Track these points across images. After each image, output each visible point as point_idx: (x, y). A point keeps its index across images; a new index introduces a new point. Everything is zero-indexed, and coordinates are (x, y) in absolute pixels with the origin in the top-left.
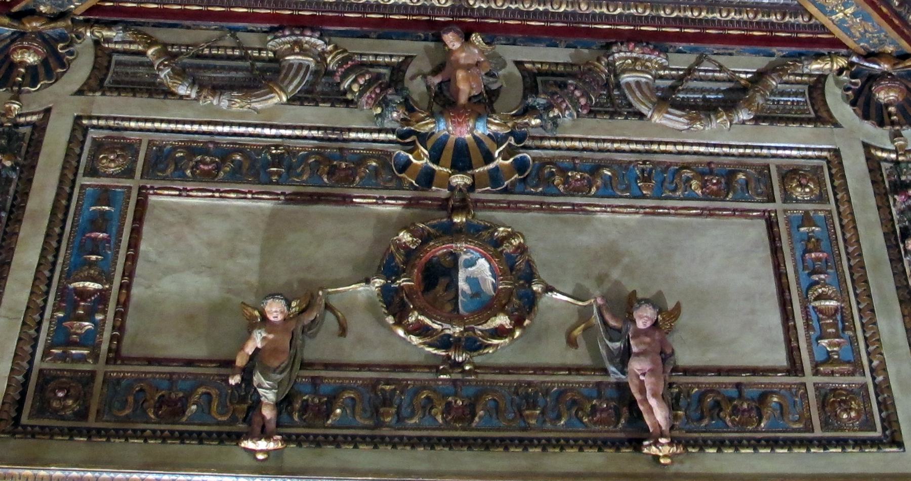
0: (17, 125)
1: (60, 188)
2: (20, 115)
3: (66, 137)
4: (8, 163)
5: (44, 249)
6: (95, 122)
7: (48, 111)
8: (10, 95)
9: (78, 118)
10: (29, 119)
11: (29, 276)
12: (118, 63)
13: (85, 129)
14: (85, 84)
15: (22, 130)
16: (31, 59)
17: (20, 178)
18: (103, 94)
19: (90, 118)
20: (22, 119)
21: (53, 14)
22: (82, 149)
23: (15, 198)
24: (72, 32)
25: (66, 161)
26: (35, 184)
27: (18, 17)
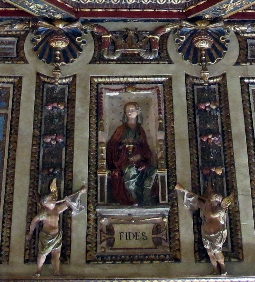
0: (210, 84)
1: (245, 120)
2: (210, 79)
3: (239, 91)
4: (214, 107)
5: (249, 156)
6: (251, 81)
7: (224, 75)
8: (201, 67)
9: (242, 79)
10: (215, 80)
11: (247, 171)
12: (252, 45)
13: (247, 84)
14: (239, 58)
15: (213, 87)
16: (205, 45)
17: (221, 115)
18: (251, 64)
19: (249, 78)
20: (211, 81)
21: (211, 18)
22: (249, 96)
23: (223, 127)
24: (225, 28)
25: (244, 105)
26: (232, 118)
27: (193, 21)
